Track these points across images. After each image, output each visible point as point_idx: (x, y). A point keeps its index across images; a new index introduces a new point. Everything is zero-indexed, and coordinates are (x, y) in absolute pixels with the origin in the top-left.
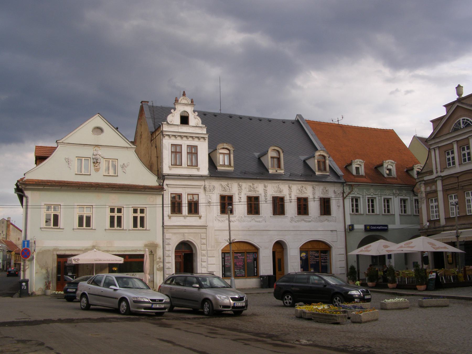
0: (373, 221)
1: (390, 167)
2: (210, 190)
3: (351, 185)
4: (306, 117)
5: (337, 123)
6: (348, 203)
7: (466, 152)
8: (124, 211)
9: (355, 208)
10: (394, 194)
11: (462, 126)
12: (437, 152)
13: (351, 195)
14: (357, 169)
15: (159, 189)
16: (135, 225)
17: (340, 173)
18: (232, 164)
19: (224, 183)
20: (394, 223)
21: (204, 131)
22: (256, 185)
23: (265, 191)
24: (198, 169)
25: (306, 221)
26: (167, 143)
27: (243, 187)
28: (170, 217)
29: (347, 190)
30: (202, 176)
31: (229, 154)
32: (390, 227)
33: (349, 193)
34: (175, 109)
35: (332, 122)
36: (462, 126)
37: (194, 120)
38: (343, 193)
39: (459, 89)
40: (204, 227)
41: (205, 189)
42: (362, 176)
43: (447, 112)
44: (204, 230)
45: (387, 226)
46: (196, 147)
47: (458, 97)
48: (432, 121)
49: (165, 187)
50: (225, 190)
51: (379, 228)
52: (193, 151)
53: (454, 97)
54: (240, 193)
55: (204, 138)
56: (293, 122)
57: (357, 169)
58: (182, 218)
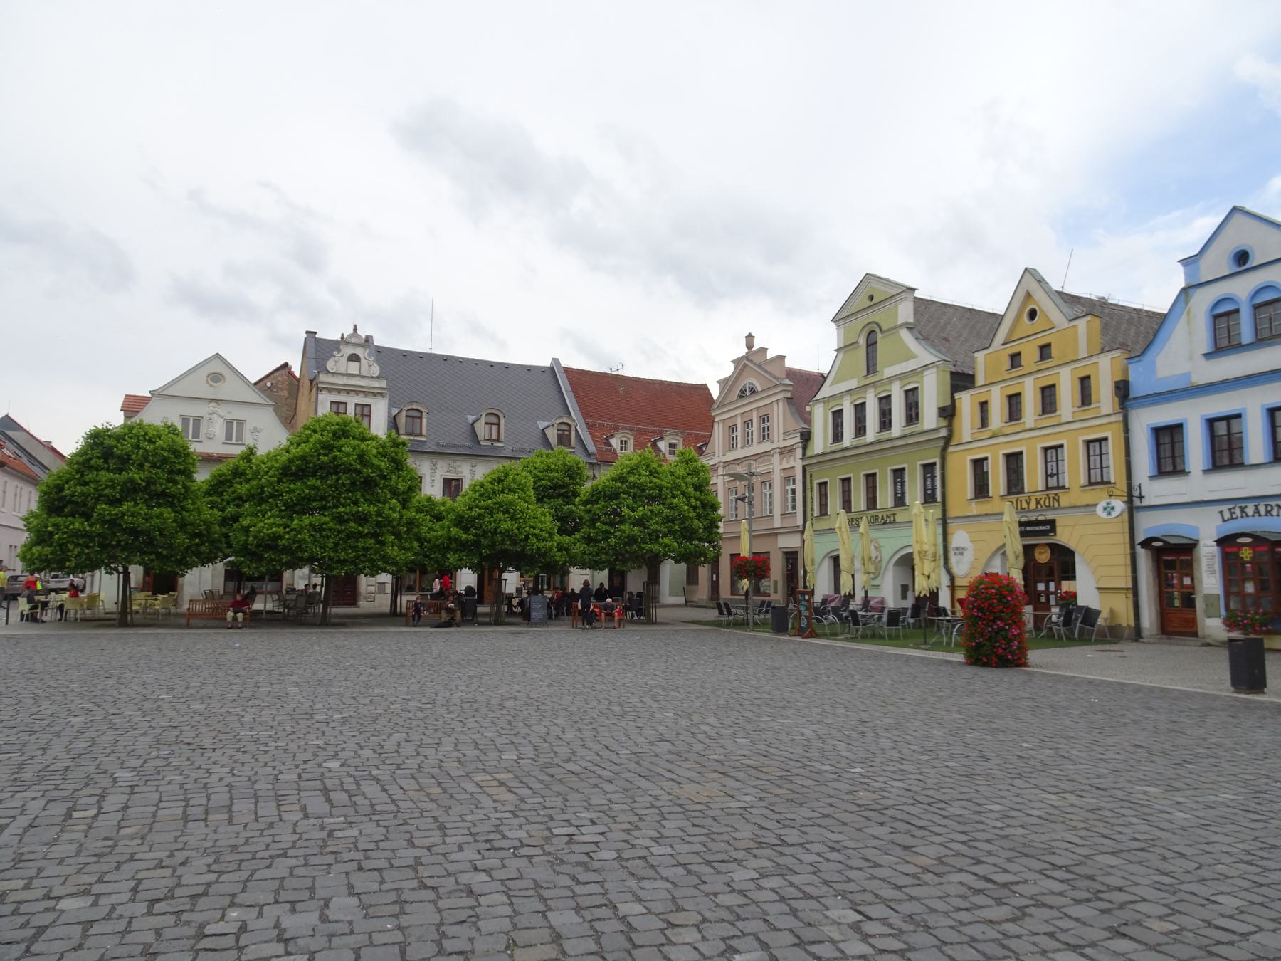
4: (563, 364)
5: (616, 373)
7: (765, 425)
11: (748, 393)
12: (721, 425)
17: (592, 448)
22: (458, 463)
27: (438, 466)
31: (421, 418)
34: (339, 351)
35: (609, 372)
36: (748, 393)
39: (750, 338)
43: (735, 368)
47: (746, 350)
48: (719, 382)
53: (743, 351)
55: (381, 394)
56: (543, 370)
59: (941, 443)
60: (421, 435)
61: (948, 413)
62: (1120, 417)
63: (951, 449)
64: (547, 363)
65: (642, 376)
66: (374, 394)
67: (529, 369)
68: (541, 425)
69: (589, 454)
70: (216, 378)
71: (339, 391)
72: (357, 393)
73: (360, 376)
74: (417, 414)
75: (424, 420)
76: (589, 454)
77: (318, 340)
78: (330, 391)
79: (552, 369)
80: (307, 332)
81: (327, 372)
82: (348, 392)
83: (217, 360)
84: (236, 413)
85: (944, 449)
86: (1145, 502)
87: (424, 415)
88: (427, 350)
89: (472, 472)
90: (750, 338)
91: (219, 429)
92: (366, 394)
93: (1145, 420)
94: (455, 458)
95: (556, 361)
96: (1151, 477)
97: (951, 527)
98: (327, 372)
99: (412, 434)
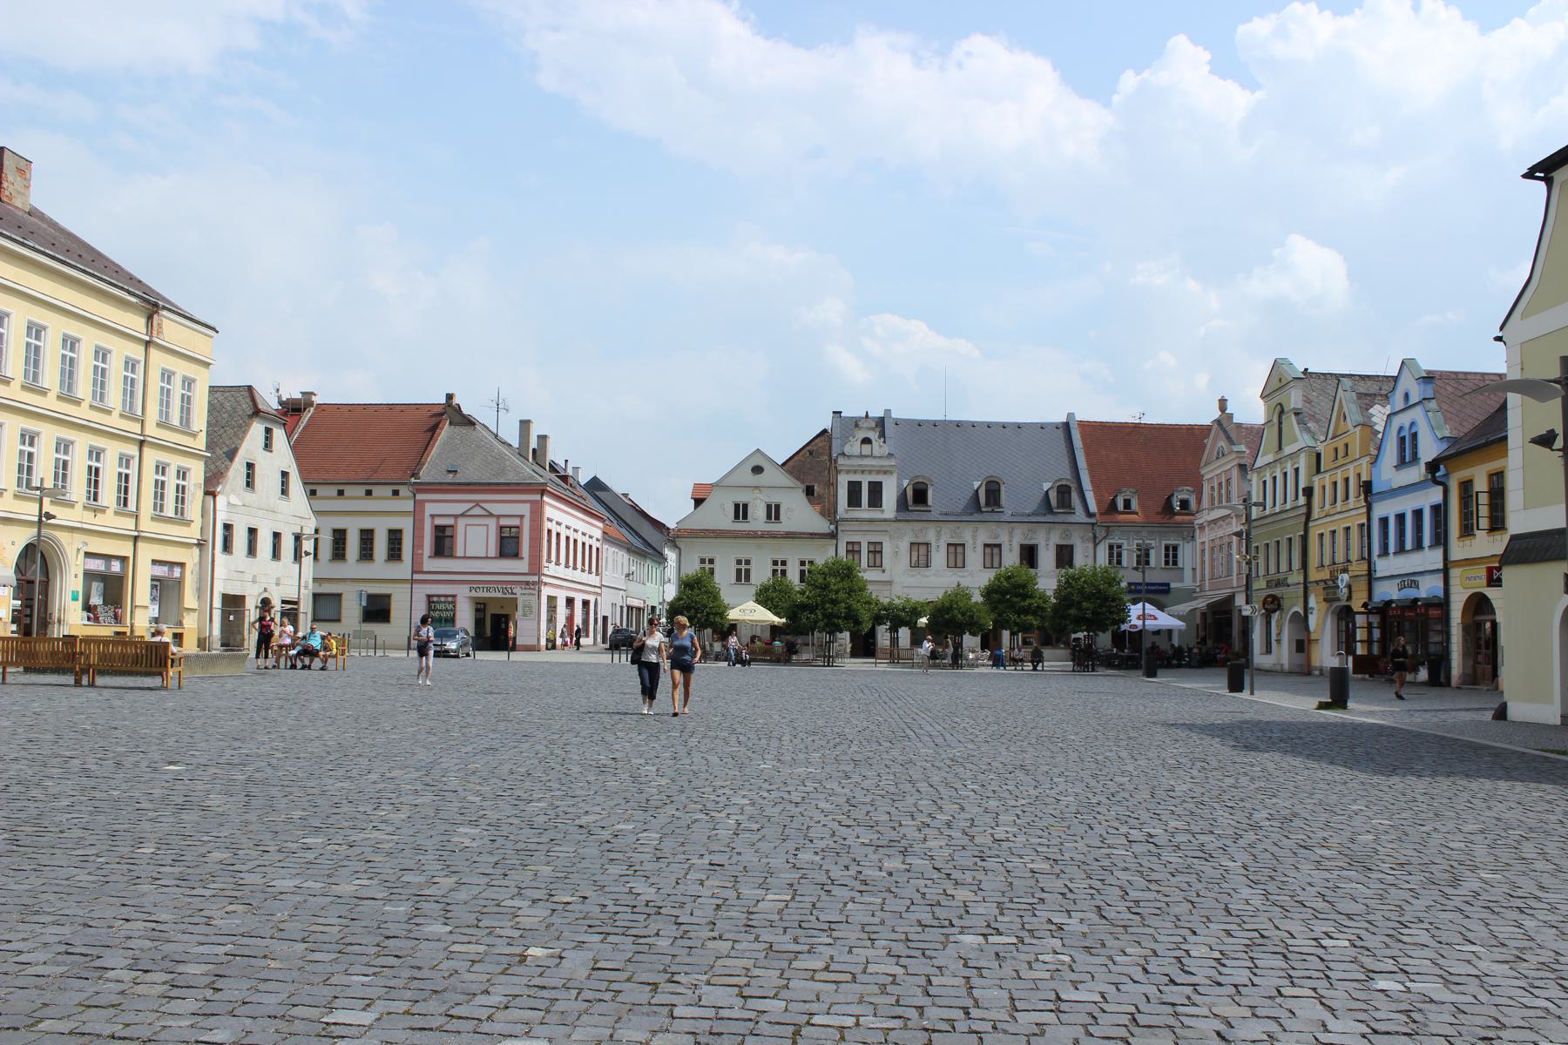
3: (1108, 527)
5: (1138, 421)
8: (789, 563)
10: (1184, 539)
14: (1127, 503)
15: (833, 536)
17: (1093, 508)
20: (1182, 580)
23: (974, 538)
26: (843, 482)
27: (943, 532)
30: (885, 520)
33: (1105, 538)
38: (1095, 537)
39: (1223, 403)
40: (890, 583)
44: (888, 587)
45: (1168, 585)
49: (840, 535)
50: (916, 537)
52: (876, 489)
54: (938, 540)
57: (1127, 503)
59: (1303, 519)
61: (1308, 492)
62: (1364, 510)
63: (1311, 524)
65: (1167, 422)
66: (885, 472)
69: (1090, 515)
70: (757, 470)
71: (855, 472)
73: (871, 456)
76: (1090, 515)
78: (848, 472)
79: (1066, 426)
80: (834, 412)
82: (863, 472)
83: (758, 455)
84: (774, 498)
85: (1306, 524)
86: (1379, 574)
88: (941, 418)
89: (974, 538)
90: (1223, 403)
92: (878, 472)
93: (1382, 509)
95: (1071, 415)
96: (1379, 556)
97: (1311, 587)
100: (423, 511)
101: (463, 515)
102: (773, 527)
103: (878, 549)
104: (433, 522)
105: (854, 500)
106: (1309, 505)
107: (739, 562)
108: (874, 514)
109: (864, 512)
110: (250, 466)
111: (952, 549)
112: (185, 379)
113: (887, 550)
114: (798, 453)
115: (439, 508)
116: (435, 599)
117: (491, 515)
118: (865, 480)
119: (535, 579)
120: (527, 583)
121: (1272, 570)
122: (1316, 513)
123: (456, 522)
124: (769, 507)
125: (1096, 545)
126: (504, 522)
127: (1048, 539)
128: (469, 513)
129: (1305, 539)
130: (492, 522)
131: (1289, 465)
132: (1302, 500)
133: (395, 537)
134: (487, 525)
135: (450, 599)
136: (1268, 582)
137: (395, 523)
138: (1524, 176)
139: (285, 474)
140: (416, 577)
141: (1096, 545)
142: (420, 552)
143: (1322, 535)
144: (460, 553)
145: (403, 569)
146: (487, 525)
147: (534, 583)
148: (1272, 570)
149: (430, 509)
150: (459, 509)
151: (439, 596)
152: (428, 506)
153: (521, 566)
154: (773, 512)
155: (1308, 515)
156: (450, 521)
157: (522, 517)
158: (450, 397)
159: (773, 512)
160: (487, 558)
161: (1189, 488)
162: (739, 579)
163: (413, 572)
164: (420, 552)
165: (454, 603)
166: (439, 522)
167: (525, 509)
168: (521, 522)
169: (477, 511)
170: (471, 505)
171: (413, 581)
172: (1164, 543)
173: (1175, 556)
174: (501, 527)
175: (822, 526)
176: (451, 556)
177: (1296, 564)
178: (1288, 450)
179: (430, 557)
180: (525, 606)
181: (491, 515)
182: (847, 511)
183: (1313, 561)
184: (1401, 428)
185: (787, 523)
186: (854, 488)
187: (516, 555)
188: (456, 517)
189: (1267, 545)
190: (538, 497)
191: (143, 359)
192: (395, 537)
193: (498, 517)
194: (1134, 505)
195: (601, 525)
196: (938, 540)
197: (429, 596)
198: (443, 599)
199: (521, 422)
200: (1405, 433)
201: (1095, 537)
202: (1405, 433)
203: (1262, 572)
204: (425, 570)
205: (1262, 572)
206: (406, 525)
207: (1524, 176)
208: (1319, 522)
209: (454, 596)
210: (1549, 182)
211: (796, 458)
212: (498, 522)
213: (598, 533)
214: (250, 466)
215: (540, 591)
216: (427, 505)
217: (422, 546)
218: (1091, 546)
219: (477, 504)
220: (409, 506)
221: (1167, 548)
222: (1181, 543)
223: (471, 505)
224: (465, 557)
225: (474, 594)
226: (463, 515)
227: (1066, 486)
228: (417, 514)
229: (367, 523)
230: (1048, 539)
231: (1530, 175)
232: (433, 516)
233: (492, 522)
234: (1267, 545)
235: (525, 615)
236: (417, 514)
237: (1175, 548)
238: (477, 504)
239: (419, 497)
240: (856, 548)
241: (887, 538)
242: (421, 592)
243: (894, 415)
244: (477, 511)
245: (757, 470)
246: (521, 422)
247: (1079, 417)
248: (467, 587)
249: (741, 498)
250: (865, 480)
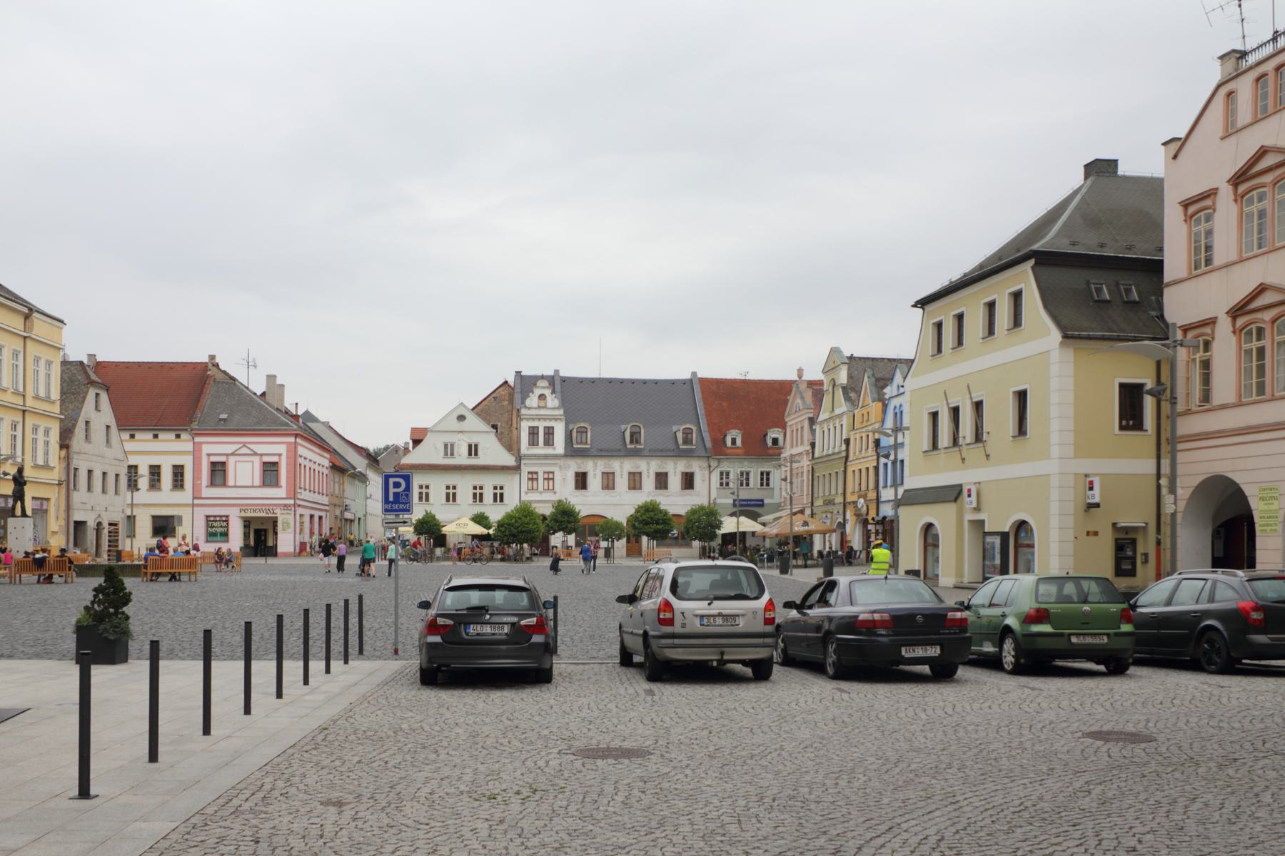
0: (745, 494)
1: (775, 436)
2: (565, 468)
5: (743, 378)
6: (715, 477)
9: (724, 484)
13: (719, 470)
14: (734, 441)
15: (517, 468)
16: (495, 500)
18: (589, 442)
19: (579, 461)
20: (772, 497)
21: (561, 412)
22: (611, 462)
23: (621, 467)
24: (555, 449)
25: (664, 496)
26: (525, 426)
28: (527, 493)
29: (714, 464)
31: (586, 432)
32: (766, 501)
34: (533, 393)
37: (552, 401)
38: (710, 466)
41: (560, 467)
42: (738, 448)
45: (762, 501)
46: (553, 428)
49: (523, 466)
51: (753, 503)
52: (549, 432)
54: (595, 469)
55: (560, 419)
56: (684, 382)
57: (734, 441)
58: (537, 494)
59: (844, 460)
60: (586, 443)
61: (847, 442)
62: (875, 457)
63: (848, 463)
64: (688, 376)
65: (766, 379)
66: (556, 420)
67: (673, 383)
68: (675, 428)
70: (461, 418)
72: (545, 419)
74: (583, 430)
75: (589, 434)
77: (522, 377)
78: (528, 419)
81: (526, 407)
82: (539, 419)
83: (462, 407)
84: (474, 439)
85: (845, 464)
87: (589, 430)
89: (621, 467)
91: (465, 451)
94: (609, 458)
97: (848, 506)
98: (526, 407)
99: (581, 443)
100: (200, 451)
101: (233, 454)
102: (473, 461)
103: (551, 476)
104: (209, 459)
105: (533, 441)
106: (847, 450)
107: (448, 488)
108: (549, 451)
109: (541, 450)
110: (87, 423)
111: (605, 475)
112: (47, 361)
113: (558, 477)
114: (485, 399)
115: (215, 447)
116: (212, 519)
117: (255, 454)
118: (541, 425)
119: (292, 502)
120: (285, 505)
121: (827, 493)
122: (851, 458)
123: (228, 459)
124: (470, 446)
125: (710, 472)
126: (266, 459)
127: (675, 468)
128: (237, 452)
129: (845, 472)
130: (257, 460)
131: (837, 422)
132: (844, 447)
133: (178, 472)
134: (253, 462)
135: (224, 519)
136: (824, 501)
137: (178, 461)
138: (913, 306)
139: (108, 427)
140: (196, 502)
141: (710, 472)
142: (199, 482)
143: (854, 471)
144: (231, 482)
145: (185, 496)
146: (253, 462)
147: (290, 505)
148: (827, 493)
149: (206, 449)
150: (230, 449)
151: (215, 516)
152: (204, 446)
153: (280, 492)
154: (473, 450)
155: (847, 457)
156: (222, 459)
157: (280, 455)
158: (212, 357)
159: (473, 450)
160: (253, 486)
161: (780, 430)
162: (448, 500)
163: (194, 498)
164: (199, 482)
165: (227, 521)
166: (214, 459)
167: (282, 449)
168: (280, 459)
169: (244, 451)
170: (240, 446)
171: (193, 505)
172: (760, 470)
173: (768, 479)
174: (264, 463)
175: (510, 460)
176: (224, 484)
177: (840, 490)
178: (837, 411)
179: (207, 487)
180: (283, 523)
181: (255, 454)
182: (528, 449)
183: (849, 490)
184: (895, 407)
185: (481, 460)
186: (533, 432)
187: (276, 484)
188: (227, 455)
189: (824, 475)
190: (292, 439)
191: (22, 350)
192: (178, 472)
193: (261, 455)
194: (739, 443)
195: (328, 456)
196: (595, 469)
197: (207, 517)
198: (218, 519)
199: (268, 376)
200: (897, 410)
201: (710, 466)
202: (897, 410)
203: (821, 494)
204: (203, 496)
205: (821, 494)
206: (187, 462)
207: (913, 306)
208: (853, 462)
209: (227, 516)
210: (924, 310)
211: (483, 403)
212: (261, 459)
213: (326, 463)
214: (87, 423)
215: (295, 511)
216: (204, 446)
217: (200, 478)
218: (707, 472)
219: (244, 445)
220: (189, 446)
221: (762, 474)
222: (772, 470)
223: (240, 446)
224: (235, 487)
225: (243, 514)
226: (233, 454)
227: (689, 429)
228: (196, 453)
229: (155, 461)
230: (675, 468)
231: (915, 306)
232: (209, 455)
233: (257, 460)
234: (824, 475)
235: (284, 529)
236: (196, 453)
237: (768, 474)
238: (244, 445)
239: (197, 439)
240: (535, 476)
241: (558, 468)
242: (201, 514)
243: (562, 374)
244: (244, 451)
245: (461, 418)
246: (268, 376)
247: (699, 375)
248: (237, 509)
249: (449, 439)
250: (541, 425)
